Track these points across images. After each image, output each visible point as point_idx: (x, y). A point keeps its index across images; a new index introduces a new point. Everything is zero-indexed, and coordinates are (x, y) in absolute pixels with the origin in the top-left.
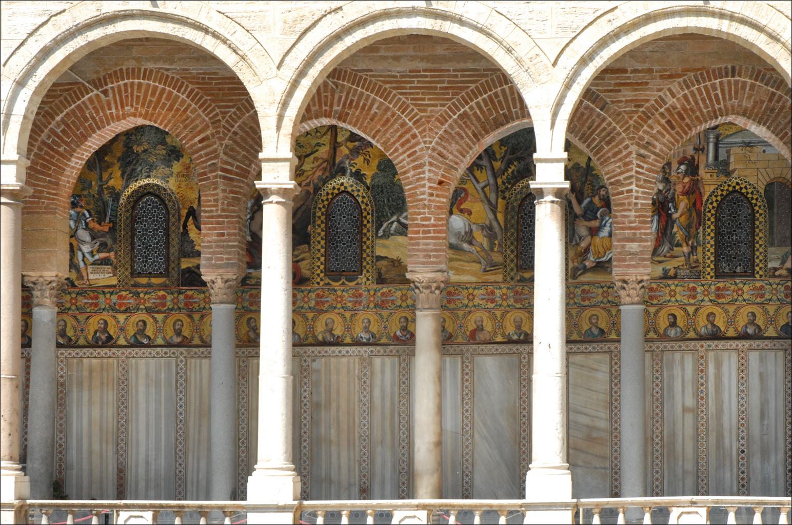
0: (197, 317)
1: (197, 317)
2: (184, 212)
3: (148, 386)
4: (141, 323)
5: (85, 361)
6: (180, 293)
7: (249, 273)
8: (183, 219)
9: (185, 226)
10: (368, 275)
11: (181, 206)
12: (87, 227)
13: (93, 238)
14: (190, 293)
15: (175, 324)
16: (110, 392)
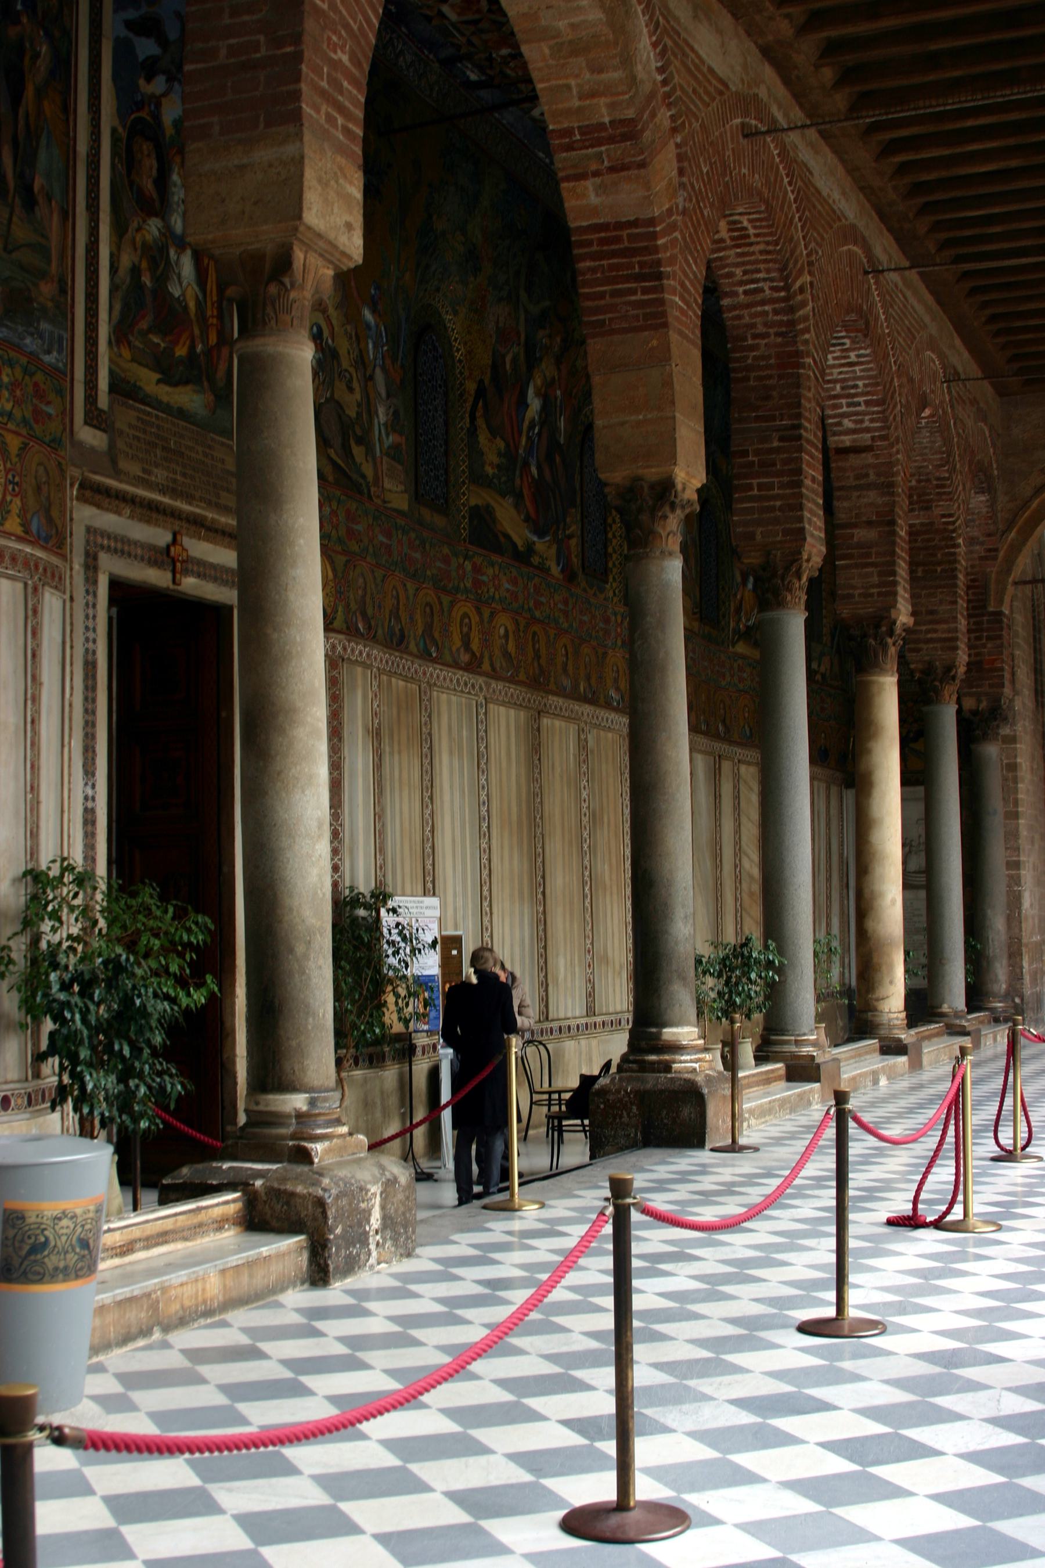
0: (486, 613)
1: (486, 613)
2: (471, 386)
3: (451, 753)
4: (428, 609)
5: (393, 680)
6: (466, 557)
7: (534, 543)
8: (468, 405)
9: (473, 418)
10: (614, 585)
11: (467, 373)
12: (384, 368)
13: (388, 396)
14: (478, 560)
15: (462, 620)
16: (416, 761)
